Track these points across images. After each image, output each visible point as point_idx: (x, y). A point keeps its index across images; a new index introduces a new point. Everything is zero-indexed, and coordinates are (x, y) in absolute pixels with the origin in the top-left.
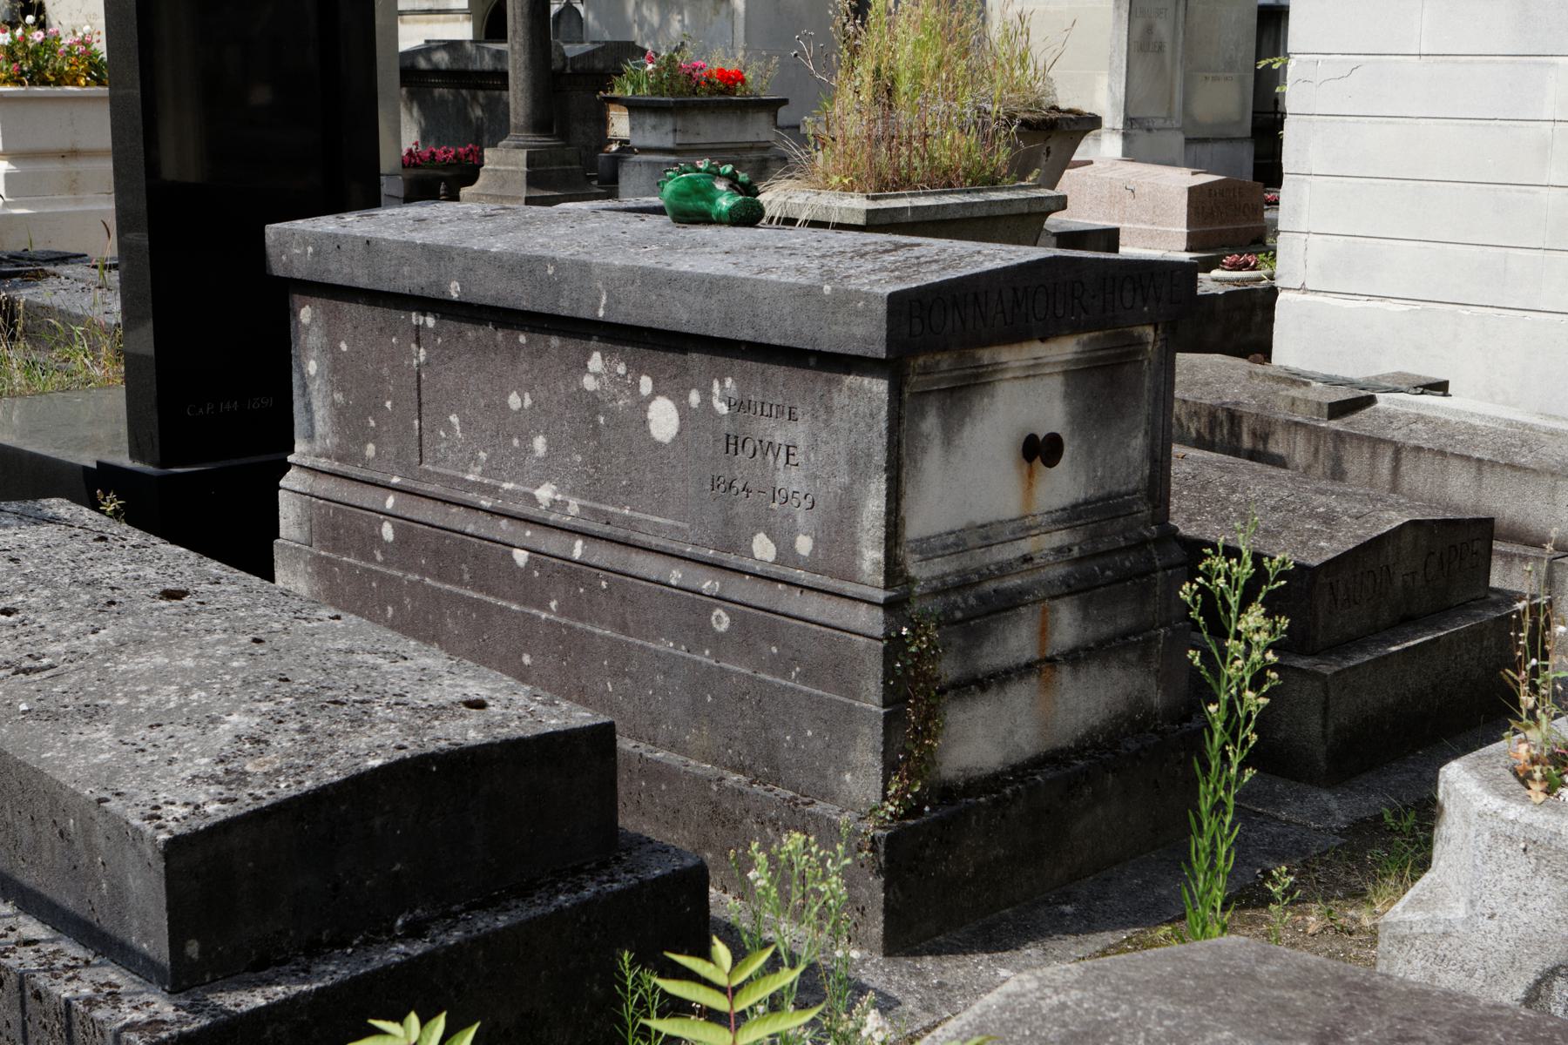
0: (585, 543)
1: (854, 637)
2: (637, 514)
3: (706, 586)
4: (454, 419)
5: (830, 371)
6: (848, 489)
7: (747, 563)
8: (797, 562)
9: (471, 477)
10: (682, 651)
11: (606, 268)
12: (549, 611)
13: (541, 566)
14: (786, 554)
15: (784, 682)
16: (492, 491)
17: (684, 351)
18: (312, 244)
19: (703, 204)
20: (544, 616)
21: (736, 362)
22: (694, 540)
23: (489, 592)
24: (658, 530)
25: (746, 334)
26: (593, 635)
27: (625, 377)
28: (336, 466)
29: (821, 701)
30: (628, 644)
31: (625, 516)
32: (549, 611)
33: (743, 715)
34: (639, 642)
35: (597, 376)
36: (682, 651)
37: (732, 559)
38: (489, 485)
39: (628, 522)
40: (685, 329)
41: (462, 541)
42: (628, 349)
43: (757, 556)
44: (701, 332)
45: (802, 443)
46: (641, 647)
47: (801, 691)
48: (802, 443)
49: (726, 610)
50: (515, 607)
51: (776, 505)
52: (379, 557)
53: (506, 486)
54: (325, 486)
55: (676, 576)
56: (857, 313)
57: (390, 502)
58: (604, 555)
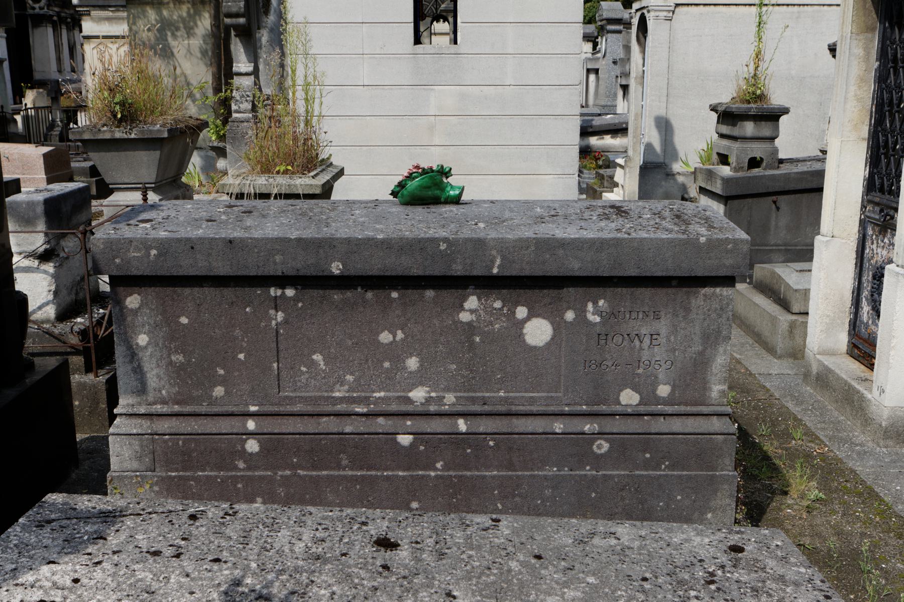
0: (254, 420)
1: (713, 437)
2: (511, 394)
3: (587, 428)
4: (317, 357)
5: (689, 287)
6: (701, 353)
7: (618, 408)
8: (658, 401)
9: (337, 394)
10: (566, 471)
11: (502, 241)
12: (436, 469)
13: (422, 442)
14: (649, 397)
15: (658, 473)
16: (365, 400)
17: (560, 287)
18: (155, 248)
19: (438, 192)
20: (433, 474)
21: (608, 290)
22: (568, 402)
23: (369, 469)
24: (532, 401)
25: (633, 272)
26: (485, 476)
27: (501, 309)
28: (176, 408)
29: (689, 478)
30: (518, 476)
31: (501, 397)
32: (436, 469)
33: (623, 499)
34: (528, 473)
35: (472, 311)
36: (566, 471)
37: (604, 408)
38: (359, 397)
39: (505, 400)
40: (577, 274)
41: (341, 439)
42: (504, 291)
43: (623, 403)
44: (593, 274)
45: (664, 331)
46: (531, 476)
47: (672, 476)
48: (664, 331)
49: (606, 440)
50: (401, 473)
51: (640, 371)
52: (241, 465)
53: (377, 395)
54: (144, 426)
55: (558, 426)
56: (727, 251)
57: (251, 425)
58: (484, 425)
